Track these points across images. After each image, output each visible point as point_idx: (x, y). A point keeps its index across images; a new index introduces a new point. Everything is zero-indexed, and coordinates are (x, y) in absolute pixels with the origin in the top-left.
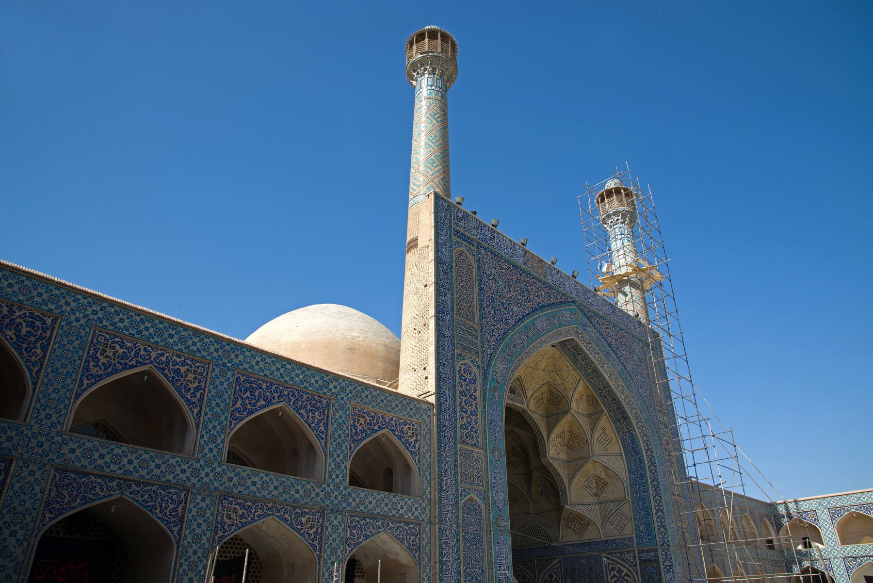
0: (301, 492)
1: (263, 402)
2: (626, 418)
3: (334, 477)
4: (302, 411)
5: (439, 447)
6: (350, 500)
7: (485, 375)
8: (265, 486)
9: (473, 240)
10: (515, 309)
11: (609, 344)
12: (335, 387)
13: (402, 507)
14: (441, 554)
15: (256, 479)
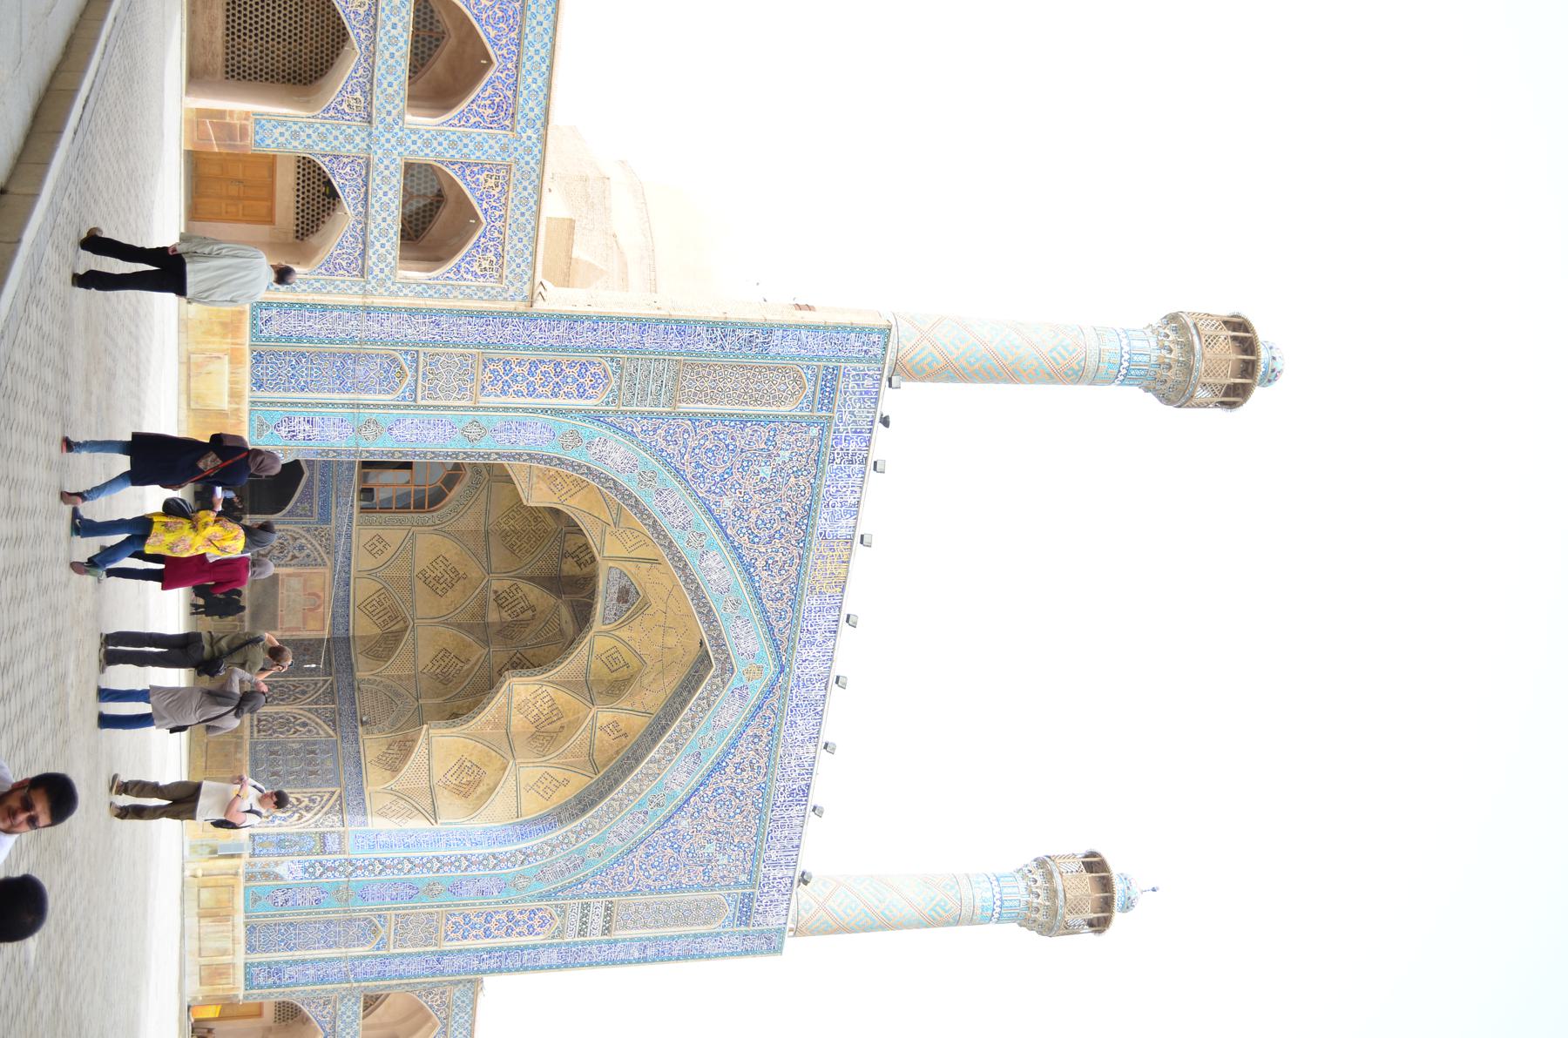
0: (390, 91)
1: (493, 33)
2: (584, 811)
3: (414, 137)
4: (490, 90)
5: (470, 314)
6: (386, 162)
7: (596, 417)
8: (393, 41)
9: (831, 410)
10: (727, 503)
11: (718, 766)
12: (529, 138)
13: (383, 246)
14: (325, 308)
15: (399, 29)
